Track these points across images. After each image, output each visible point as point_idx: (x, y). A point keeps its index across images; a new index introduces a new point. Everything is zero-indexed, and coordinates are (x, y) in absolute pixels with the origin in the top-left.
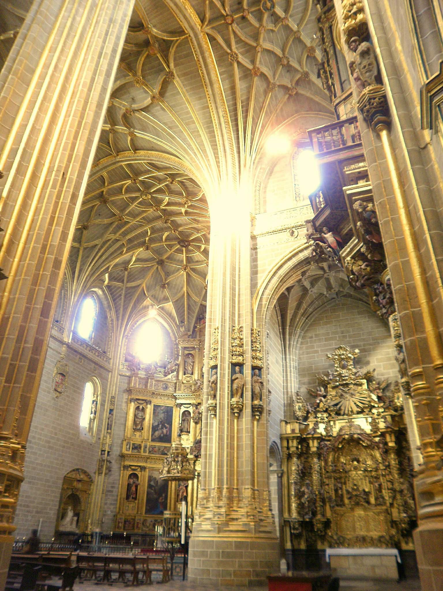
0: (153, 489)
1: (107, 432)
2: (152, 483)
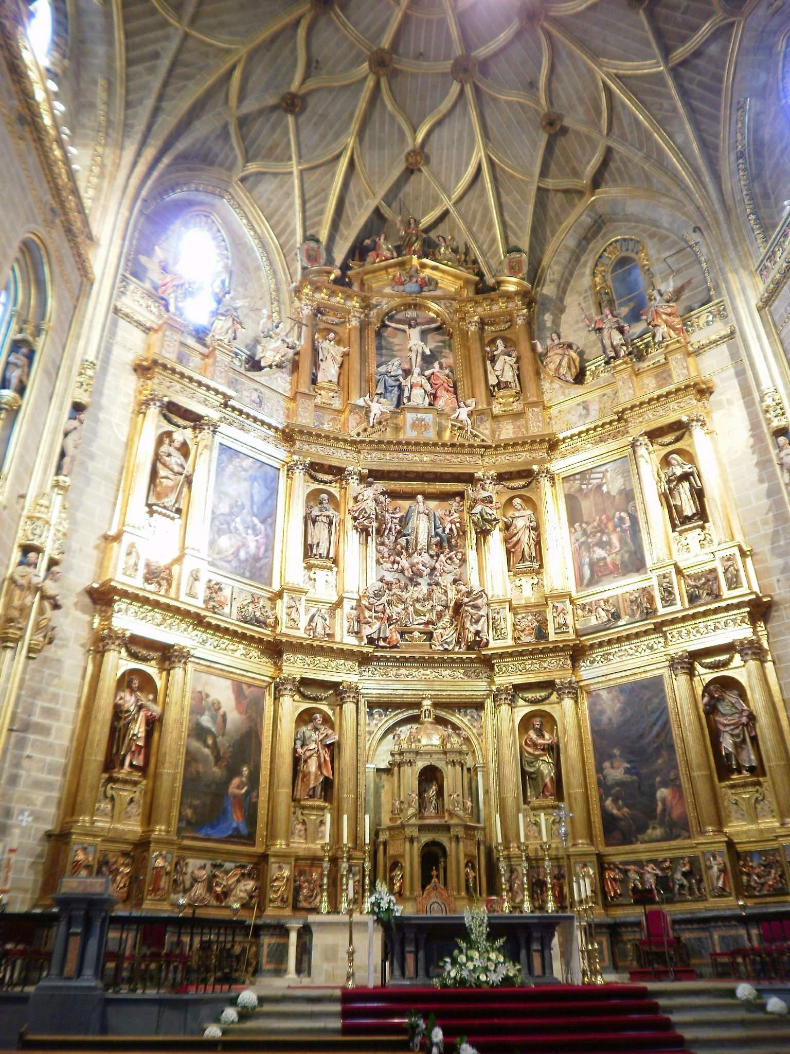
0: (210, 742)
1: (57, 485)
2: (206, 720)
